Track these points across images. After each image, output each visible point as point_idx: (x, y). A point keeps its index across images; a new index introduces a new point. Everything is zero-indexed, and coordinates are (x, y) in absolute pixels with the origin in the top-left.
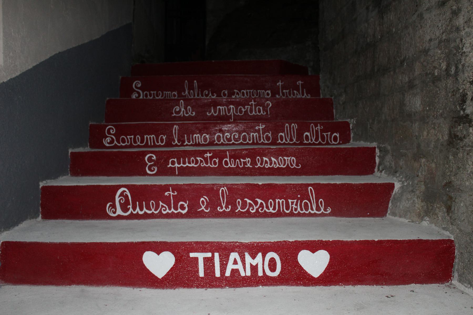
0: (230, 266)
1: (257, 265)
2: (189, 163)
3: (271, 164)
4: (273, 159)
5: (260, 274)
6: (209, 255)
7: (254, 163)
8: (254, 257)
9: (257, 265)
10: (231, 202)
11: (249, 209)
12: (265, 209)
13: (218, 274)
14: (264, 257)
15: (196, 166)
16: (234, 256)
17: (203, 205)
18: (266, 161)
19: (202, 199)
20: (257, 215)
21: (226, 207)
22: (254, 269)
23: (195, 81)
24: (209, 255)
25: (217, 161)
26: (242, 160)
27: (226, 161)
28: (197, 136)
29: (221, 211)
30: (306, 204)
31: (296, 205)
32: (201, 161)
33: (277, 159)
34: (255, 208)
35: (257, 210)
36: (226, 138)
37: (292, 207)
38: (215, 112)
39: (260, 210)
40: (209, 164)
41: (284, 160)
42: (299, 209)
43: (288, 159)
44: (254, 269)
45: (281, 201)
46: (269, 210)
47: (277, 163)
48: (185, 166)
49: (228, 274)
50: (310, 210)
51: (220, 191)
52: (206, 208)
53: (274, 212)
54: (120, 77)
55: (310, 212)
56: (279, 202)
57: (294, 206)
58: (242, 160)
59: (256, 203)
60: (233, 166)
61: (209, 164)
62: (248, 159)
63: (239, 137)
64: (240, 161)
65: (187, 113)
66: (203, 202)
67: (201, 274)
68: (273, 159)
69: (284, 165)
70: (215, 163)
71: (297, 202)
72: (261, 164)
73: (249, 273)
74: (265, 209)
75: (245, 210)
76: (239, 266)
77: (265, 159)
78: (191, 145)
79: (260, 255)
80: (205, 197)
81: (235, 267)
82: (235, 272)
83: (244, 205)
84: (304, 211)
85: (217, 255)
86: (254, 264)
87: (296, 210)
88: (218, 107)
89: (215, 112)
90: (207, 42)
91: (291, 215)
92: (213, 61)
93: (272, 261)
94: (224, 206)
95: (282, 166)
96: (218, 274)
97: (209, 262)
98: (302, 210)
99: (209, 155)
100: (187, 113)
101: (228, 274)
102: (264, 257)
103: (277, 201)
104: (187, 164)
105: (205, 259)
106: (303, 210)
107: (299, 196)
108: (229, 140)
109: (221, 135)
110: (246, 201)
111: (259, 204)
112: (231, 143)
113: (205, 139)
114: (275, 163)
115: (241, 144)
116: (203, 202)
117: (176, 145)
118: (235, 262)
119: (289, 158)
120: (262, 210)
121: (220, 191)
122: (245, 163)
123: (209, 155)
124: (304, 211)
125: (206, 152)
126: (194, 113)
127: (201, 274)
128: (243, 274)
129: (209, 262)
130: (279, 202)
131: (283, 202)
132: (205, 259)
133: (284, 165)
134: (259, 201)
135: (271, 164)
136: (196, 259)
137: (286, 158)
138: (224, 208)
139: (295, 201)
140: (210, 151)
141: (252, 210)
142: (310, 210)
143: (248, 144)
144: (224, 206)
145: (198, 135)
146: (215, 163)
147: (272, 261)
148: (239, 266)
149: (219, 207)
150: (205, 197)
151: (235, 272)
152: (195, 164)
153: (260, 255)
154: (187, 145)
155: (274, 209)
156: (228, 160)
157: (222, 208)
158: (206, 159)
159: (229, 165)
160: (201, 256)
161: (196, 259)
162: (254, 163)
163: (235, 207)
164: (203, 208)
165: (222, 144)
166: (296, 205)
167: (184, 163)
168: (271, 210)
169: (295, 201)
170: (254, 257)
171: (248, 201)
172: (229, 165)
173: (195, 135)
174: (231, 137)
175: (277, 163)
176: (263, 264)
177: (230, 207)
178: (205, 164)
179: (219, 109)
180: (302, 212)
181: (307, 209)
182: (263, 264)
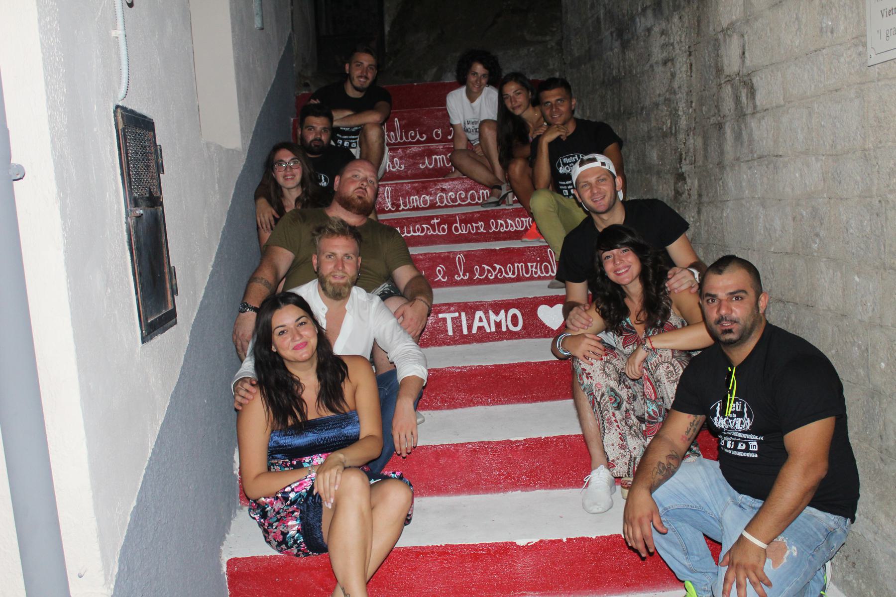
0: (476, 324)
1: (501, 321)
2: (414, 232)
3: (507, 227)
4: (509, 221)
5: (504, 329)
6: (457, 314)
7: (488, 226)
8: (497, 313)
9: (501, 321)
10: (469, 269)
11: (487, 275)
12: (504, 274)
13: (465, 332)
14: (506, 312)
15: (422, 234)
16: (479, 314)
17: (440, 274)
18: (501, 224)
19: (438, 268)
20: (496, 281)
21: (464, 275)
22: (498, 325)
23: (396, 119)
24: (457, 314)
25: (446, 227)
26: (474, 225)
27: (456, 227)
28: (414, 198)
29: (459, 279)
30: (546, 267)
31: (536, 268)
32: (428, 229)
33: (514, 221)
34: (494, 274)
35: (496, 275)
36: (451, 198)
37: (532, 271)
38: (430, 164)
39: (498, 276)
40: (437, 231)
41: (522, 221)
42: (539, 272)
43: (526, 221)
44: (498, 325)
45: (520, 265)
46: (508, 275)
47: (514, 225)
48: (409, 235)
49: (474, 331)
50: (550, 273)
51: (457, 259)
52: (443, 277)
53: (513, 277)
54: (292, 119)
55: (550, 275)
56: (518, 266)
57: (534, 269)
58: (474, 225)
59: (494, 269)
60: (464, 232)
61: (437, 231)
62: (480, 223)
63: (466, 197)
64: (472, 226)
65: (394, 167)
66: (439, 271)
67: (450, 333)
68: (509, 221)
69: (522, 227)
70: (444, 230)
71: (537, 265)
72: (496, 228)
73: (493, 329)
74: (504, 274)
75: (484, 277)
76: (485, 323)
77: (499, 221)
78: (409, 210)
79: (503, 312)
80: (442, 266)
81: (481, 324)
82: (480, 328)
83: (482, 271)
84: (545, 274)
85: (463, 314)
86: (498, 321)
87: (536, 273)
88: (434, 157)
89: (430, 164)
90: (387, 29)
91: (532, 278)
92: (415, 84)
93: (514, 317)
94: (461, 274)
95: (520, 229)
96: (465, 332)
97: (456, 322)
98: (542, 273)
99: (436, 221)
100: (394, 167)
101: (474, 331)
102: (506, 312)
103: (516, 265)
104: (412, 233)
105: (453, 319)
106: (543, 274)
107: (538, 259)
108: (454, 200)
109: (444, 195)
110: (484, 267)
111: (497, 269)
112: (457, 204)
113: (425, 202)
114: (512, 226)
115: (469, 204)
116: (439, 271)
117: (390, 211)
118: (481, 320)
119: (527, 219)
120: (500, 276)
121: (457, 259)
122: (477, 228)
123: (436, 221)
124: (545, 274)
125: (432, 218)
126: (403, 166)
127: (450, 333)
128: (488, 330)
129: (456, 322)
130: (518, 266)
131: (522, 266)
132: (453, 319)
133: (522, 227)
134: (498, 267)
135: (507, 227)
136: (445, 320)
137: (524, 219)
138: (462, 276)
139: (535, 264)
140: (437, 217)
141: (491, 276)
142: (550, 273)
143: (477, 204)
144: (461, 274)
145: (417, 197)
146: (444, 230)
147: (514, 317)
148: (485, 323)
149: (456, 276)
150: (442, 266)
151: (480, 328)
152: (421, 233)
153: (503, 312)
154: (403, 210)
155: (513, 274)
156: (458, 225)
157: (459, 276)
158: (433, 226)
159: (460, 231)
160: (448, 316)
161: (445, 320)
162: (488, 226)
163: (472, 273)
164: (440, 277)
165: (446, 206)
166: (536, 268)
167: (409, 232)
168: (510, 275)
169: (535, 264)
170: (497, 313)
171: (486, 267)
172: (460, 231)
173: (412, 198)
174: (456, 197)
175: (514, 225)
176: (506, 320)
177: (468, 274)
178: (432, 232)
179: (436, 159)
180: (542, 275)
181: (547, 272)
182: (506, 320)
